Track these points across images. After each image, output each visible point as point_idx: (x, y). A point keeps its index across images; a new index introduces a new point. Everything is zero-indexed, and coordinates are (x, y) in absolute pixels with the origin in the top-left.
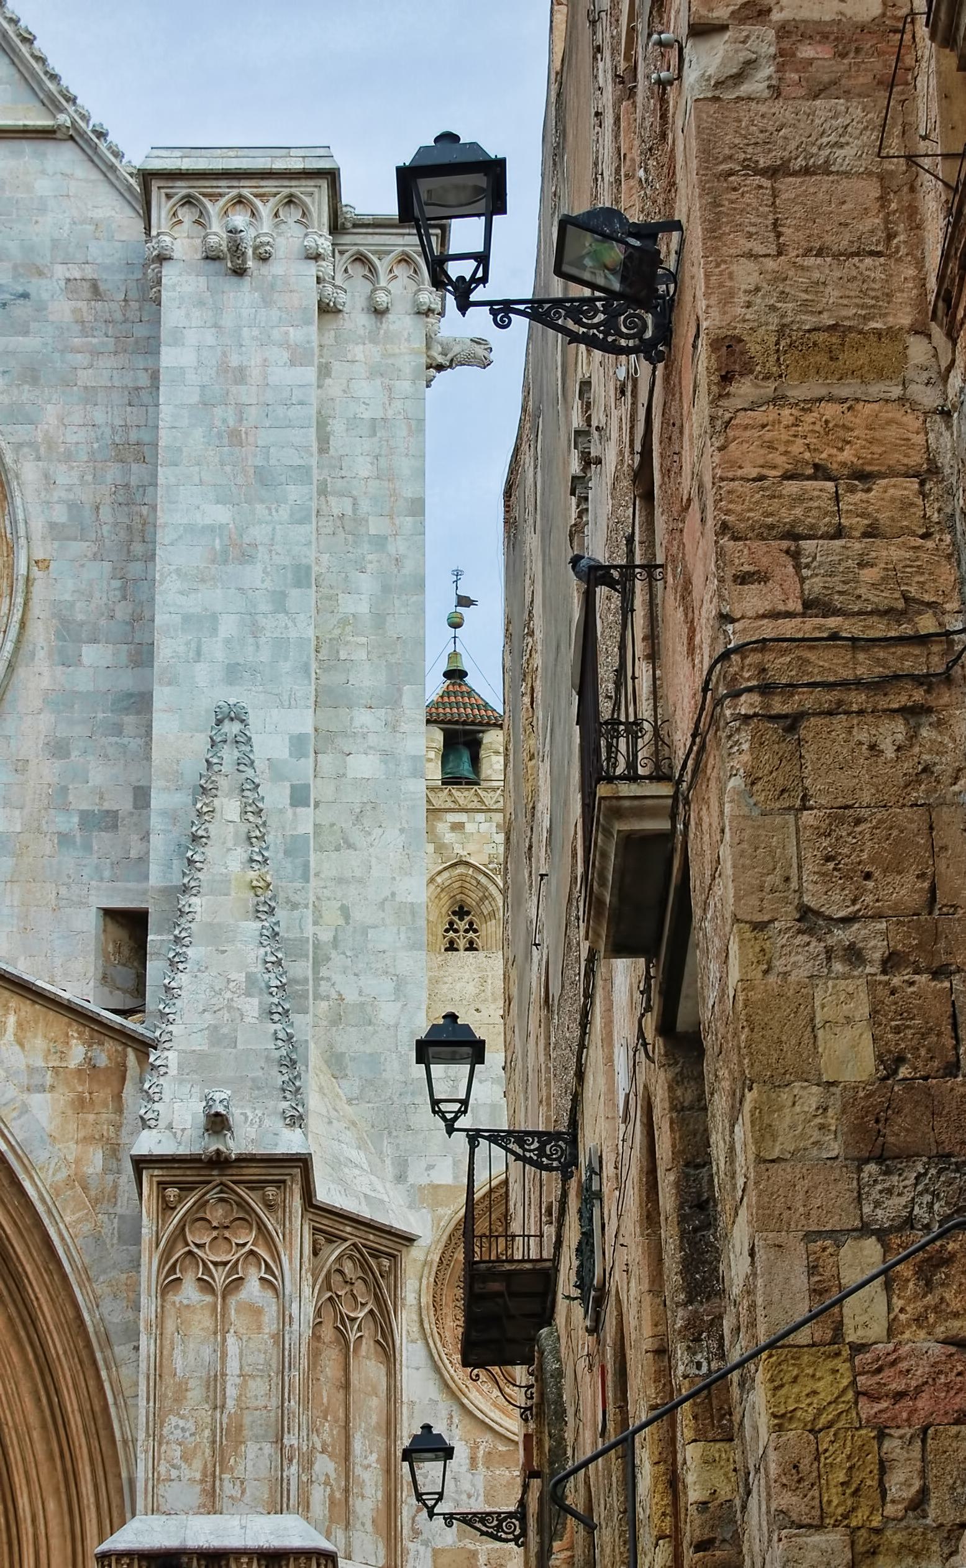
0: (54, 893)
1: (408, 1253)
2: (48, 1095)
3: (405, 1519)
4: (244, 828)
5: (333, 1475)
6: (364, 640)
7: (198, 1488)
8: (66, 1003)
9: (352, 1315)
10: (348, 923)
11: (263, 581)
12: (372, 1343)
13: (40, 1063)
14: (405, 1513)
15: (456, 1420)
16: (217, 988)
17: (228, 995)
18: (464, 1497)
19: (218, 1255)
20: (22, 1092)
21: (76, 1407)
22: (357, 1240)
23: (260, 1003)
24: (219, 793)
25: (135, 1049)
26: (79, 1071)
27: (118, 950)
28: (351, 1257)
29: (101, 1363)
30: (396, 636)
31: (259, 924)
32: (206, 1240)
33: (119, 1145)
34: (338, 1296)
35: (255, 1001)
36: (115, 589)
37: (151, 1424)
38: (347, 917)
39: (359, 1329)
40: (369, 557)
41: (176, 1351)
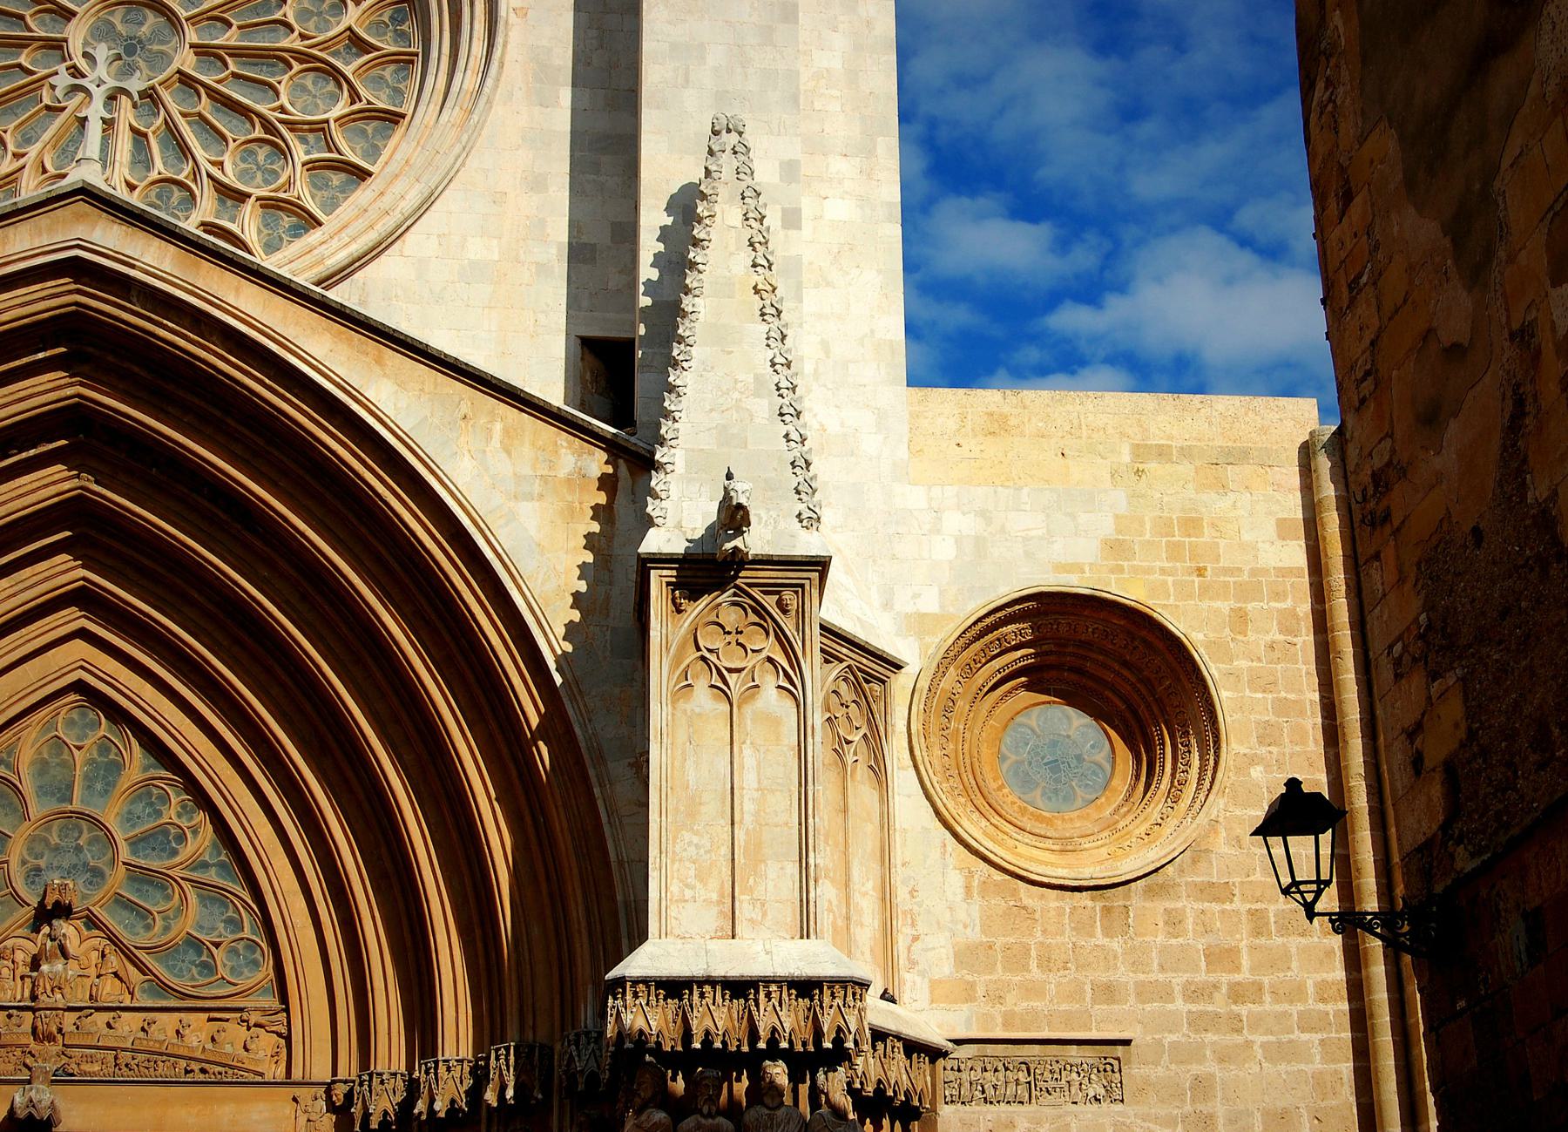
0: (532, 321)
1: (896, 679)
2: (538, 504)
3: (901, 949)
4: (747, 233)
5: (835, 902)
6: (838, 94)
7: (715, 910)
8: (555, 410)
9: (849, 738)
10: (828, 357)
11: (750, 16)
12: (866, 768)
13: (528, 471)
14: (900, 944)
15: (949, 849)
16: (724, 389)
17: (736, 395)
18: (960, 927)
19: (732, 661)
20: (510, 500)
21: (566, 826)
22: (852, 662)
23: (770, 404)
24: (719, 199)
25: (626, 461)
26: (569, 481)
27: (595, 379)
28: (845, 679)
29: (594, 780)
30: (868, 91)
31: (765, 327)
32: (718, 644)
33: (611, 556)
34: (836, 718)
35: (765, 402)
36: (592, 38)
37: (664, 840)
38: (827, 352)
39: (855, 753)
40: (841, 18)
41: (688, 762)
